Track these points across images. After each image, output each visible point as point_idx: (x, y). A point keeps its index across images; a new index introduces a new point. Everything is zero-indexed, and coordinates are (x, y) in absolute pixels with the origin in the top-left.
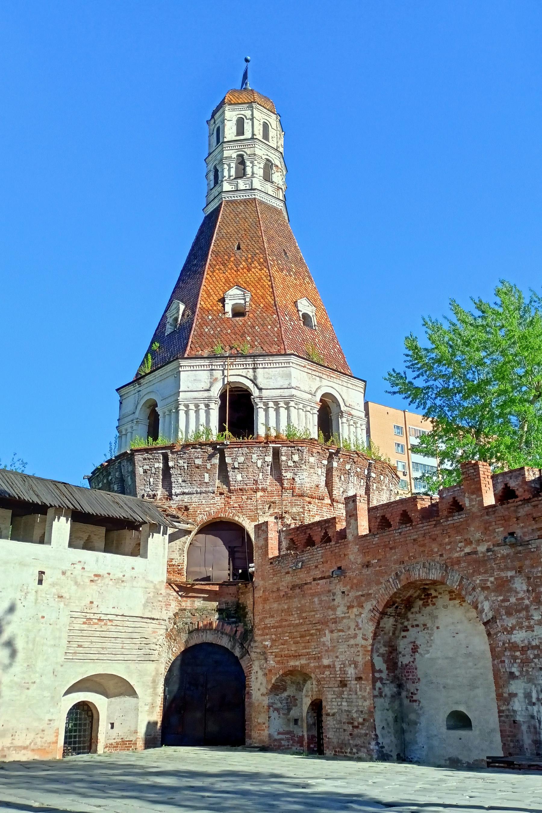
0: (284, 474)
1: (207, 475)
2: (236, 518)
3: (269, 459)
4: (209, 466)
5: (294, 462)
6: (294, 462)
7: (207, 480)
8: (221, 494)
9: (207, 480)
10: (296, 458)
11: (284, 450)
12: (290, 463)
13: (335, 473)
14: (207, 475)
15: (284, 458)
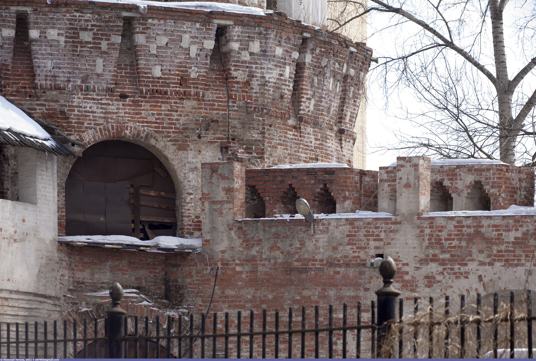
0: (234, 74)
1: (100, 62)
2: (153, 142)
3: (210, 44)
4: (104, 45)
5: (251, 54)
6: (251, 54)
7: (99, 69)
8: (123, 96)
9: (99, 69)
10: (255, 47)
11: (236, 31)
12: (246, 56)
13: (307, 73)
14: (100, 62)
15: (235, 46)
